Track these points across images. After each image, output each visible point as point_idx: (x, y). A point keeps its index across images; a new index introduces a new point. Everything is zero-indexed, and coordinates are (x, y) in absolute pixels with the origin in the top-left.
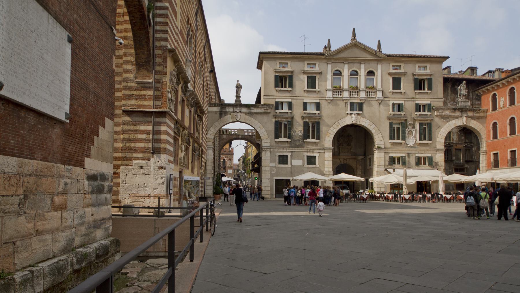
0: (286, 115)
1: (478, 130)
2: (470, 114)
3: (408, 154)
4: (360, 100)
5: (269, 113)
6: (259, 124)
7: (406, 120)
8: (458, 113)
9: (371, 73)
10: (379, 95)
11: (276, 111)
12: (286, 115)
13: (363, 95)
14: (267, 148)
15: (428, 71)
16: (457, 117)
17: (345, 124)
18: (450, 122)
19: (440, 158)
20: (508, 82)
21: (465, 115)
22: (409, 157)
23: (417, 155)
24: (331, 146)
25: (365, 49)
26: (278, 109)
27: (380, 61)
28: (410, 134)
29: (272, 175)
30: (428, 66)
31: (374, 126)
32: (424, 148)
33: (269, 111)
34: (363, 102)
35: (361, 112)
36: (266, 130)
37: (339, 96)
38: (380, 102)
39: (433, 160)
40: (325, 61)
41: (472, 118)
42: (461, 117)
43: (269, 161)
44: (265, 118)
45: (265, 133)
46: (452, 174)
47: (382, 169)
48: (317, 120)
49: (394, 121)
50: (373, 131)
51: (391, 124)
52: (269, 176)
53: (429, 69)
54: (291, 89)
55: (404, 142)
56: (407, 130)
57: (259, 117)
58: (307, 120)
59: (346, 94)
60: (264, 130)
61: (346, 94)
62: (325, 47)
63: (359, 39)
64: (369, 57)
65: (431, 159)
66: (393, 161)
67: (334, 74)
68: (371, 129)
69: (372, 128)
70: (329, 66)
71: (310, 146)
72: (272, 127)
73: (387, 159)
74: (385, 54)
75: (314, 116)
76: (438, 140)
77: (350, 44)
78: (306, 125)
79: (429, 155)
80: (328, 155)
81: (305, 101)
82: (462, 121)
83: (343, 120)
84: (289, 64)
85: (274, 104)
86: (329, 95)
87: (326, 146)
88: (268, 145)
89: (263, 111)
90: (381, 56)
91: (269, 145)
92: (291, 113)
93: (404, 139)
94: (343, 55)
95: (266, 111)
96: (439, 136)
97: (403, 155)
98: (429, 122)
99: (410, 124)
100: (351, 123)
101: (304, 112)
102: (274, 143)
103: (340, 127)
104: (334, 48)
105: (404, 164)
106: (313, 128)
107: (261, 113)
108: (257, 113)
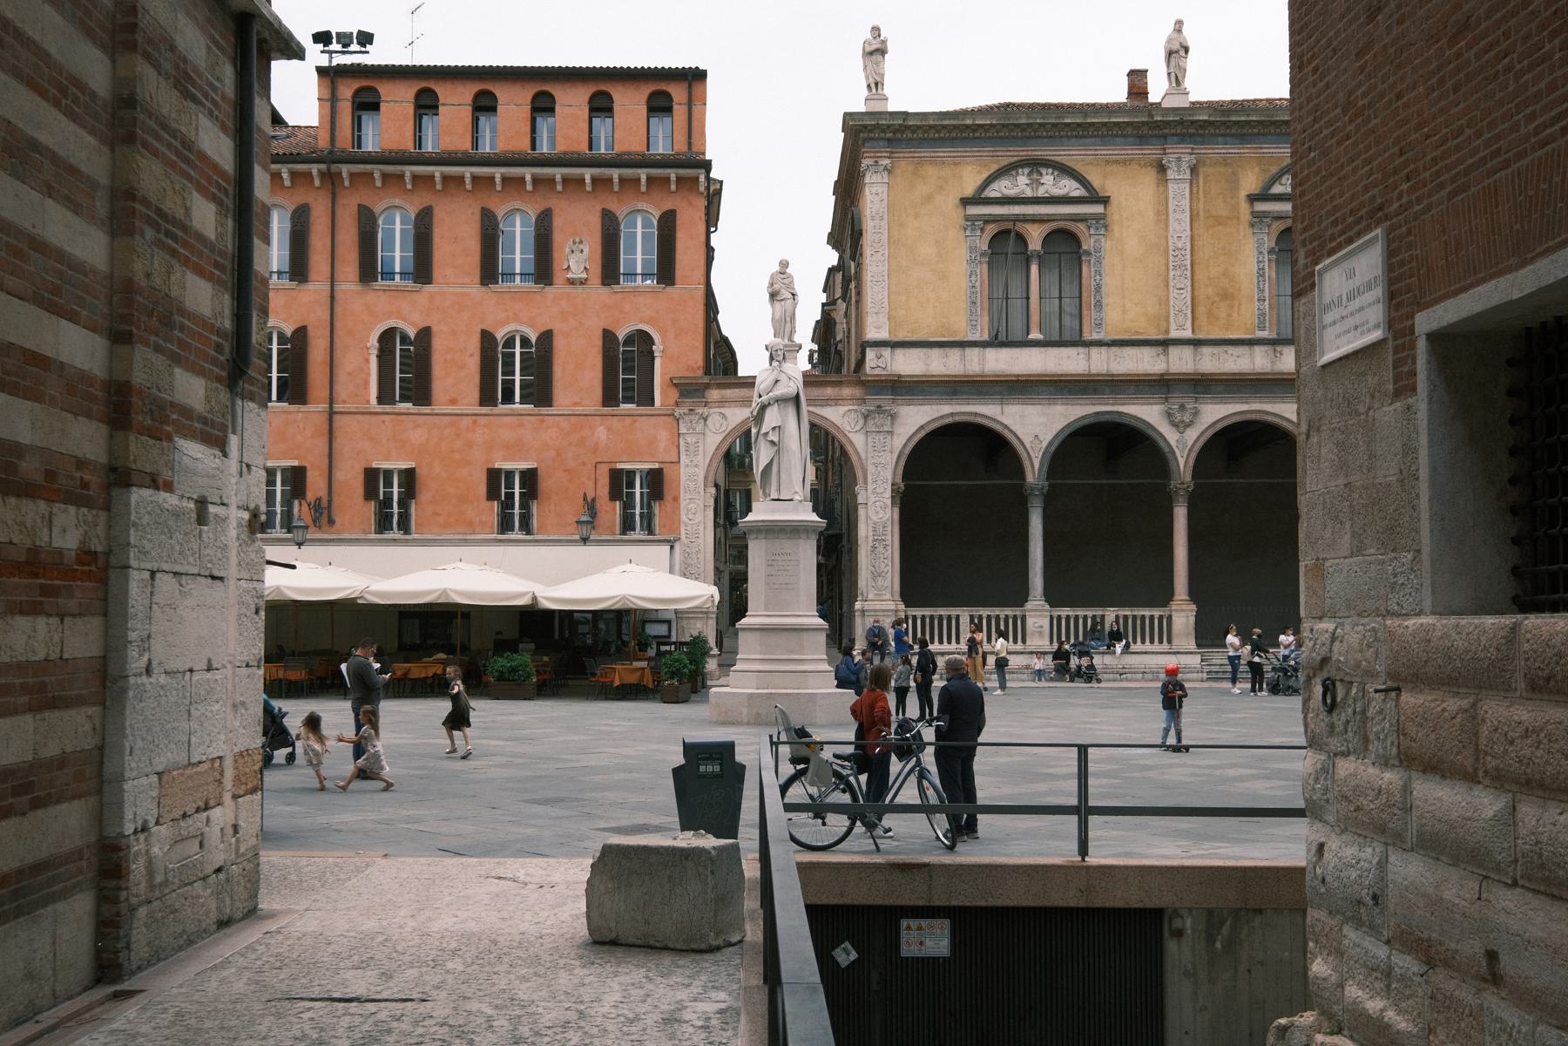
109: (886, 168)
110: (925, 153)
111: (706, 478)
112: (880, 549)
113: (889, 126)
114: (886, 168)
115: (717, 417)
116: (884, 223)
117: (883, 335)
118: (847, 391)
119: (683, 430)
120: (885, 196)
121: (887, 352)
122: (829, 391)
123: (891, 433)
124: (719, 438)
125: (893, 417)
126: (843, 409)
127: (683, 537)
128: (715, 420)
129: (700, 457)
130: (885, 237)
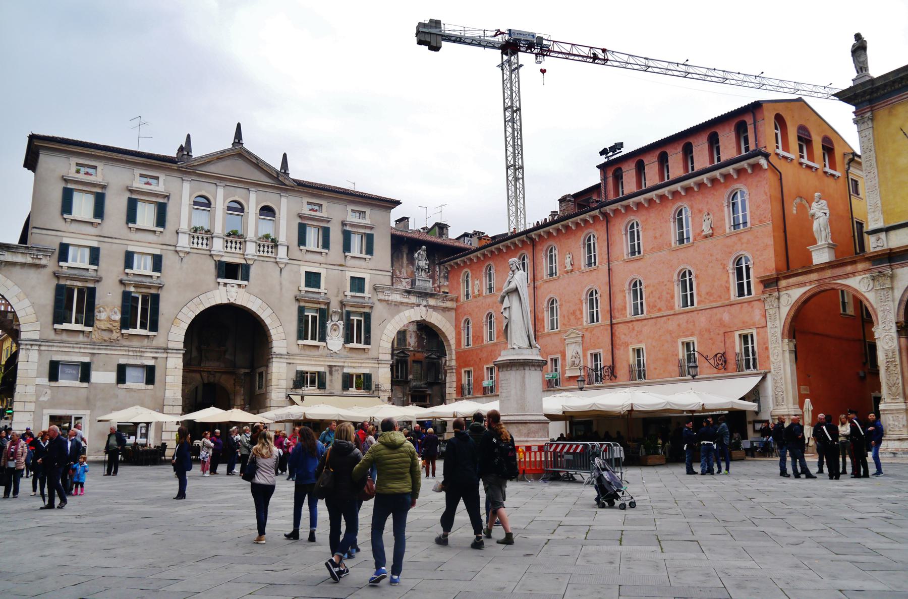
0: (84, 273)
1: (444, 330)
2: (432, 302)
3: (330, 367)
4: (245, 259)
5: (44, 266)
6: (16, 288)
7: (328, 304)
8: (413, 299)
9: (267, 211)
10: (282, 252)
11: (61, 264)
12: (84, 273)
13: (251, 249)
14: (32, 343)
15: (367, 221)
16: (412, 305)
17: (213, 303)
18: (401, 314)
19: (383, 376)
20: (484, 255)
21: (425, 303)
22: (331, 373)
23: (346, 370)
24: (181, 346)
25: (257, 164)
26: (66, 260)
27: (286, 190)
28: (335, 330)
29: (41, 406)
30: (368, 211)
31: (269, 311)
32: (358, 356)
33: (44, 262)
34: (249, 262)
35: (245, 283)
36: (33, 304)
37: (204, 247)
38: (282, 266)
39: (373, 379)
40: (176, 174)
41: (434, 308)
42: (418, 305)
43: (34, 374)
44: (32, 275)
45: (30, 310)
46: (408, 405)
47: (282, 395)
48: (153, 291)
49: (307, 305)
50: (268, 321)
51: (301, 310)
52: (31, 407)
53: (371, 216)
54: (99, 221)
55: (324, 344)
56: (329, 324)
57: (17, 270)
58: (132, 289)
59: (218, 245)
60: (27, 302)
61: (218, 245)
62: (181, 149)
63: (248, 143)
64: (264, 179)
65: (368, 377)
66: (301, 380)
67: (195, 203)
68: (263, 317)
69: (265, 315)
70: (187, 186)
71: (135, 343)
72: (47, 298)
73: (293, 375)
74: (294, 180)
75: (148, 281)
76: (383, 344)
77: (230, 150)
78: (128, 302)
79: (367, 371)
80: (175, 364)
81: (130, 249)
82: (416, 314)
83: (209, 294)
84: (99, 169)
85: (57, 247)
86: (184, 241)
87: (171, 345)
88: (36, 336)
89: (29, 260)
90: (287, 182)
91: (38, 338)
92: (96, 270)
93: (323, 339)
94: (213, 169)
95: (37, 261)
96: (384, 337)
97: (321, 369)
98: (367, 310)
99: (335, 312)
100: (225, 301)
101: (127, 271)
102: (53, 332)
103: (202, 308)
104: (196, 152)
105: (322, 386)
106: (141, 310)
107: (23, 265)
108: (14, 264)
109: (869, 119)
110: (894, 99)
111: (783, 334)
112: (892, 368)
113: (865, 92)
114: (869, 119)
115: (785, 296)
116: (873, 153)
117: (880, 225)
118: (860, 266)
119: (767, 307)
120: (871, 136)
121: (883, 235)
122: (849, 269)
123: (892, 288)
124: (788, 308)
125: (892, 277)
126: (858, 278)
127: (772, 370)
128: (784, 299)
129: (778, 322)
130: (874, 162)
